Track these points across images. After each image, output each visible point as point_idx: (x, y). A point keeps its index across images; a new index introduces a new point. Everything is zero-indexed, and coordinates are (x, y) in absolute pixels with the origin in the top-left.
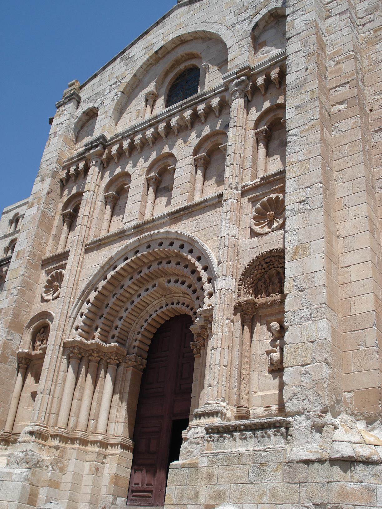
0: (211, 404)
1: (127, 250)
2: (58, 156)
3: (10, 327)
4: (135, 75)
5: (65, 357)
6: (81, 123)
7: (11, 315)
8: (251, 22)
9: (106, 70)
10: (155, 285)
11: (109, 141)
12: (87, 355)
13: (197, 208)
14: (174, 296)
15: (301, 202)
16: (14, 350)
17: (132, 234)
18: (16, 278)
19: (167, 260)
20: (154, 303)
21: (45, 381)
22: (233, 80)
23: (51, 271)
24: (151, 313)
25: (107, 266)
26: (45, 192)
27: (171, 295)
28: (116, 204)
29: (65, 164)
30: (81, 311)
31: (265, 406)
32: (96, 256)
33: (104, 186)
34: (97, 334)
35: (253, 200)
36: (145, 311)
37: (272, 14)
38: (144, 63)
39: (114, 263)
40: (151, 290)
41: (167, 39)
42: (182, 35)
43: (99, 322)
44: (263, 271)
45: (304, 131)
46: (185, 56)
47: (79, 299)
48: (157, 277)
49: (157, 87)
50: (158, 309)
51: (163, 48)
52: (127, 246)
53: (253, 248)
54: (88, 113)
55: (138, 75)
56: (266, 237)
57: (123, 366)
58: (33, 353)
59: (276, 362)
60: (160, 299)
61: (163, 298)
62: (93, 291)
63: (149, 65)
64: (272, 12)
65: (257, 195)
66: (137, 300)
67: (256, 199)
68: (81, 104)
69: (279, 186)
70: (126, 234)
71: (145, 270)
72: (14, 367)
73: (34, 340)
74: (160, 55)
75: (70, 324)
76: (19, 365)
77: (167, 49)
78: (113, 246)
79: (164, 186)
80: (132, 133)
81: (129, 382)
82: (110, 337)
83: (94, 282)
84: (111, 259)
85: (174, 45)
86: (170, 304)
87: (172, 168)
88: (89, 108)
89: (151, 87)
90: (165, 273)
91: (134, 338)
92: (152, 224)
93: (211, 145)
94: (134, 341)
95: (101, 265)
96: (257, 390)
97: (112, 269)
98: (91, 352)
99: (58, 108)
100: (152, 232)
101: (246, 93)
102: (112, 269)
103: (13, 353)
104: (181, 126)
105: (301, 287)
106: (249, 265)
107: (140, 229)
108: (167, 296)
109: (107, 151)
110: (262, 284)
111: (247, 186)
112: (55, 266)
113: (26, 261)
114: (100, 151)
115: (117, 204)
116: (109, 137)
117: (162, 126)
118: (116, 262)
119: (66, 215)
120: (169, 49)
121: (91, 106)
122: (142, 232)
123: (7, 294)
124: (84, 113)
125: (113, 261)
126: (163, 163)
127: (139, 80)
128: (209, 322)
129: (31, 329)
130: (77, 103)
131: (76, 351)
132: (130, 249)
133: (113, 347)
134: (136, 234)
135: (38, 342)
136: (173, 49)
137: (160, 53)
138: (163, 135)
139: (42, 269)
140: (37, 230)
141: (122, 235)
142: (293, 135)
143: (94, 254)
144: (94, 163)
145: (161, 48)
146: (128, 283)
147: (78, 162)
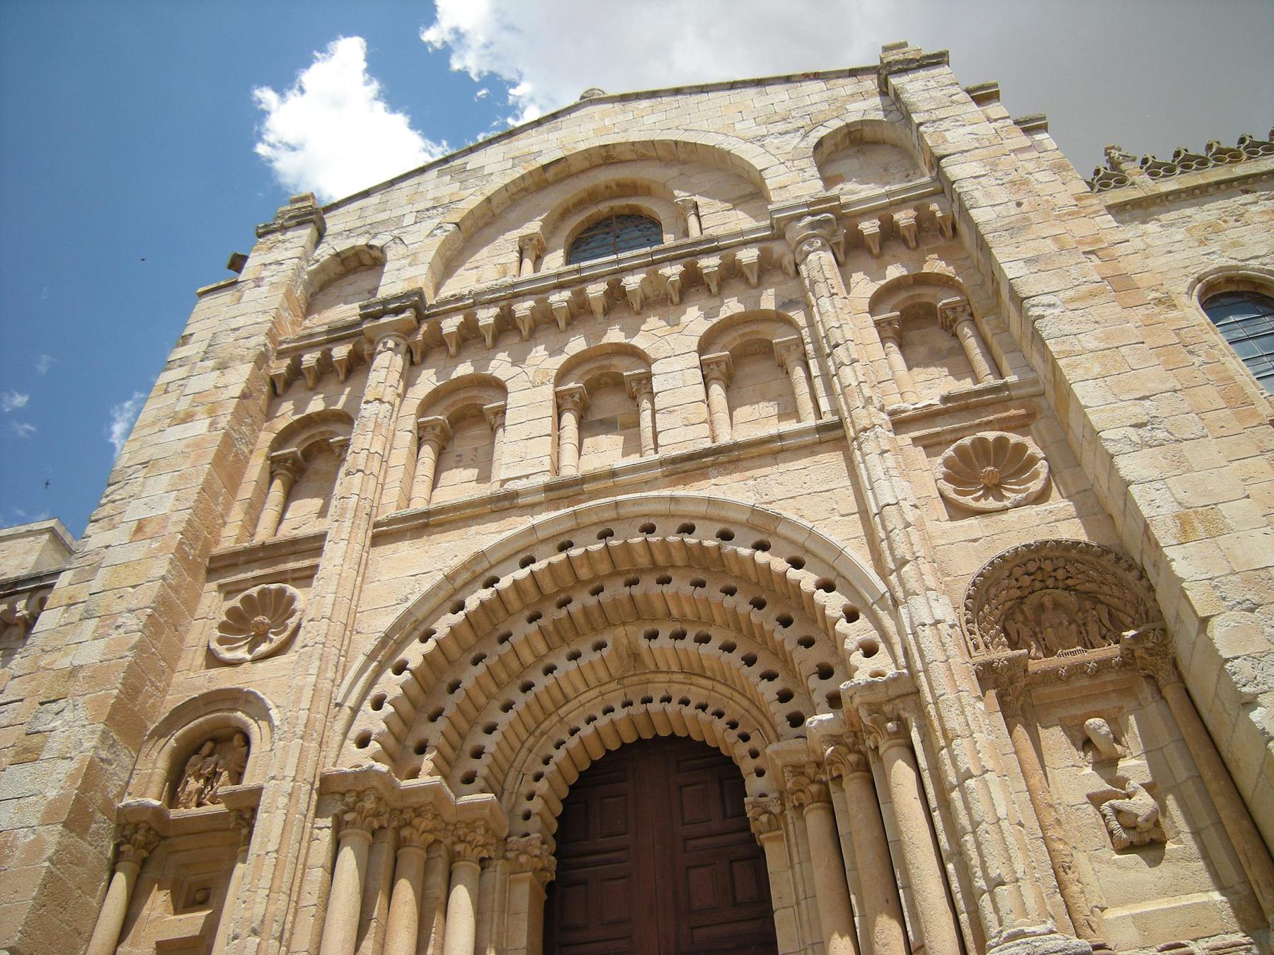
0: (1034, 934)
1: (533, 539)
2: (273, 323)
3: (110, 719)
4: (489, 200)
5: (328, 822)
6: (323, 277)
7: (120, 686)
8: (806, 135)
9: (397, 186)
10: (599, 646)
11: (432, 306)
12: (395, 824)
13: (755, 451)
14: (649, 682)
15: (1139, 426)
16: (111, 796)
17: (540, 503)
18: (133, 587)
19: (657, 575)
20: (583, 698)
21: (267, 892)
22: (800, 217)
23: (242, 586)
24: (574, 725)
25: (466, 576)
26: (236, 391)
27: (643, 678)
28: (444, 448)
29: (285, 346)
30: (376, 691)
31: (1162, 945)
32: (412, 552)
33: (419, 402)
34: (427, 762)
35: (925, 442)
36: (555, 718)
37: (850, 133)
38: (513, 182)
39: (487, 570)
40: (589, 656)
41: (574, 148)
42: (614, 145)
43: (433, 732)
44: (1018, 593)
45: (1072, 300)
46: (614, 187)
47: (371, 657)
48: (609, 624)
49: (551, 227)
50: (599, 714)
51: (563, 164)
52: (533, 528)
53: (975, 540)
54: (347, 258)
55: (495, 202)
56: (1004, 517)
57: (499, 868)
58: (174, 814)
59: (1147, 820)
60: (603, 689)
61: (613, 685)
62: (417, 640)
63: (522, 190)
64: (853, 129)
65: (938, 434)
66: (542, 682)
67: (936, 440)
68: (327, 239)
69: (995, 416)
70: (520, 501)
71: (582, 600)
72: (101, 853)
73: (176, 777)
74: (550, 175)
75: (340, 726)
76: (122, 848)
77: (569, 167)
78: (474, 529)
79: (599, 417)
80: (506, 297)
81: (524, 916)
82: (459, 780)
83: (420, 615)
84: (480, 556)
85: (587, 164)
86: (637, 703)
87: (634, 374)
88: (353, 247)
89: (533, 227)
90: (637, 611)
91: (525, 790)
92: (610, 483)
93: (738, 341)
94: (523, 799)
95: (447, 571)
96: (1104, 904)
97: (480, 583)
98: (408, 815)
99: (260, 236)
100: (620, 498)
101: (834, 246)
102: (480, 583)
103: (107, 807)
104: (646, 298)
105: (1244, 601)
106: (981, 575)
107: (570, 491)
108: (626, 682)
109: (424, 327)
110: (1019, 625)
111: (904, 411)
112: (258, 573)
113: (175, 544)
114: (410, 322)
115: (449, 449)
116: (430, 300)
117: (596, 290)
118: (492, 567)
119: (279, 461)
120: (573, 170)
121: (362, 241)
122: (573, 499)
123: (97, 628)
124: (338, 255)
125: (485, 565)
126: (598, 368)
127: (494, 215)
128: (883, 718)
129: (172, 740)
130: (316, 234)
131: (369, 804)
132: (541, 535)
133: (482, 805)
134: (553, 503)
135: (192, 780)
136: (583, 171)
137: (552, 171)
138: (598, 308)
139: (208, 580)
140: (209, 474)
141: (506, 504)
142: (1043, 306)
143: (404, 549)
144: (391, 344)
145: (558, 161)
146: (522, 630)
147: (329, 346)
